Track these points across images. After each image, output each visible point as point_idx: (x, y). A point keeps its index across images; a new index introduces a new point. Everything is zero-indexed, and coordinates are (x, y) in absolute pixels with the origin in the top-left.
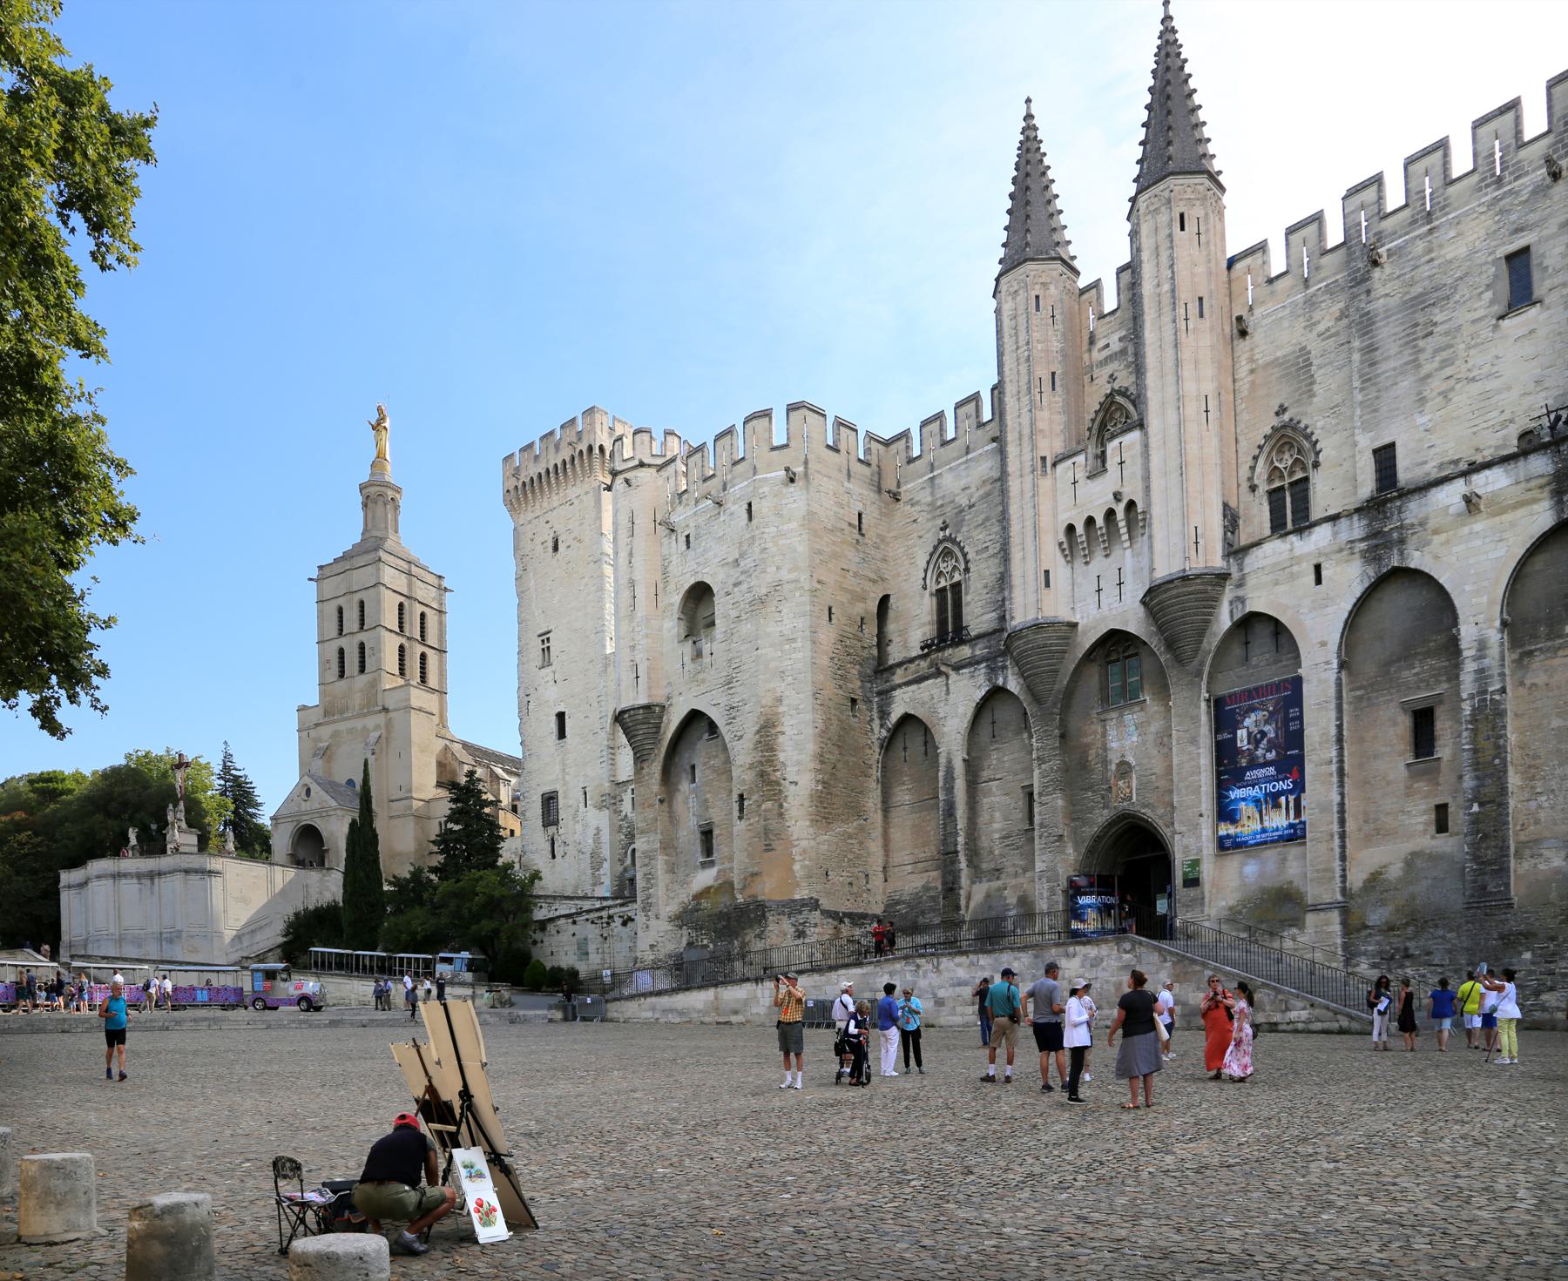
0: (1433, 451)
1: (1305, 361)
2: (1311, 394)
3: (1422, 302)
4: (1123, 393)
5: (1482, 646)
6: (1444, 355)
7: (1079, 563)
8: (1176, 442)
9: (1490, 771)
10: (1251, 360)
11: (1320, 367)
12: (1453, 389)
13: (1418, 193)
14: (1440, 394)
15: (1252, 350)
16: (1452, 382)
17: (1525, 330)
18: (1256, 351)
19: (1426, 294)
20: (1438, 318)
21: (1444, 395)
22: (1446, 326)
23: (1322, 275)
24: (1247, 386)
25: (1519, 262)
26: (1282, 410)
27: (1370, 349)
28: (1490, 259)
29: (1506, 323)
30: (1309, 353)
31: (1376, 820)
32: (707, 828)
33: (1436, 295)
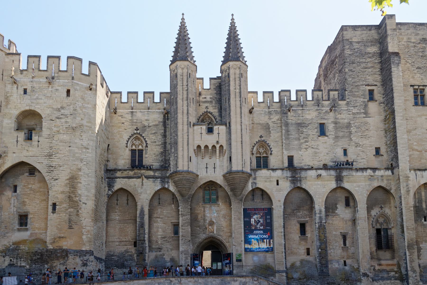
1: (268, 127)
3: (301, 125)
5: (320, 211)
6: (306, 139)
7: (200, 158)
8: (240, 134)
9: (323, 242)
10: (252, 120)
11: (272, 130)
12: (308, 148)
14: (305, 148)
15: (253, 118)
17: (324, 141)
18: (254, 119)
20: (305, 130)
21: (306, 149)
22: (306, 133)
23: (273, 107)
26: (261, 137)
27: (287, 131)
28: (317, 122)
29: (320, 138)
31: (291, 250)
32: (26, 214)
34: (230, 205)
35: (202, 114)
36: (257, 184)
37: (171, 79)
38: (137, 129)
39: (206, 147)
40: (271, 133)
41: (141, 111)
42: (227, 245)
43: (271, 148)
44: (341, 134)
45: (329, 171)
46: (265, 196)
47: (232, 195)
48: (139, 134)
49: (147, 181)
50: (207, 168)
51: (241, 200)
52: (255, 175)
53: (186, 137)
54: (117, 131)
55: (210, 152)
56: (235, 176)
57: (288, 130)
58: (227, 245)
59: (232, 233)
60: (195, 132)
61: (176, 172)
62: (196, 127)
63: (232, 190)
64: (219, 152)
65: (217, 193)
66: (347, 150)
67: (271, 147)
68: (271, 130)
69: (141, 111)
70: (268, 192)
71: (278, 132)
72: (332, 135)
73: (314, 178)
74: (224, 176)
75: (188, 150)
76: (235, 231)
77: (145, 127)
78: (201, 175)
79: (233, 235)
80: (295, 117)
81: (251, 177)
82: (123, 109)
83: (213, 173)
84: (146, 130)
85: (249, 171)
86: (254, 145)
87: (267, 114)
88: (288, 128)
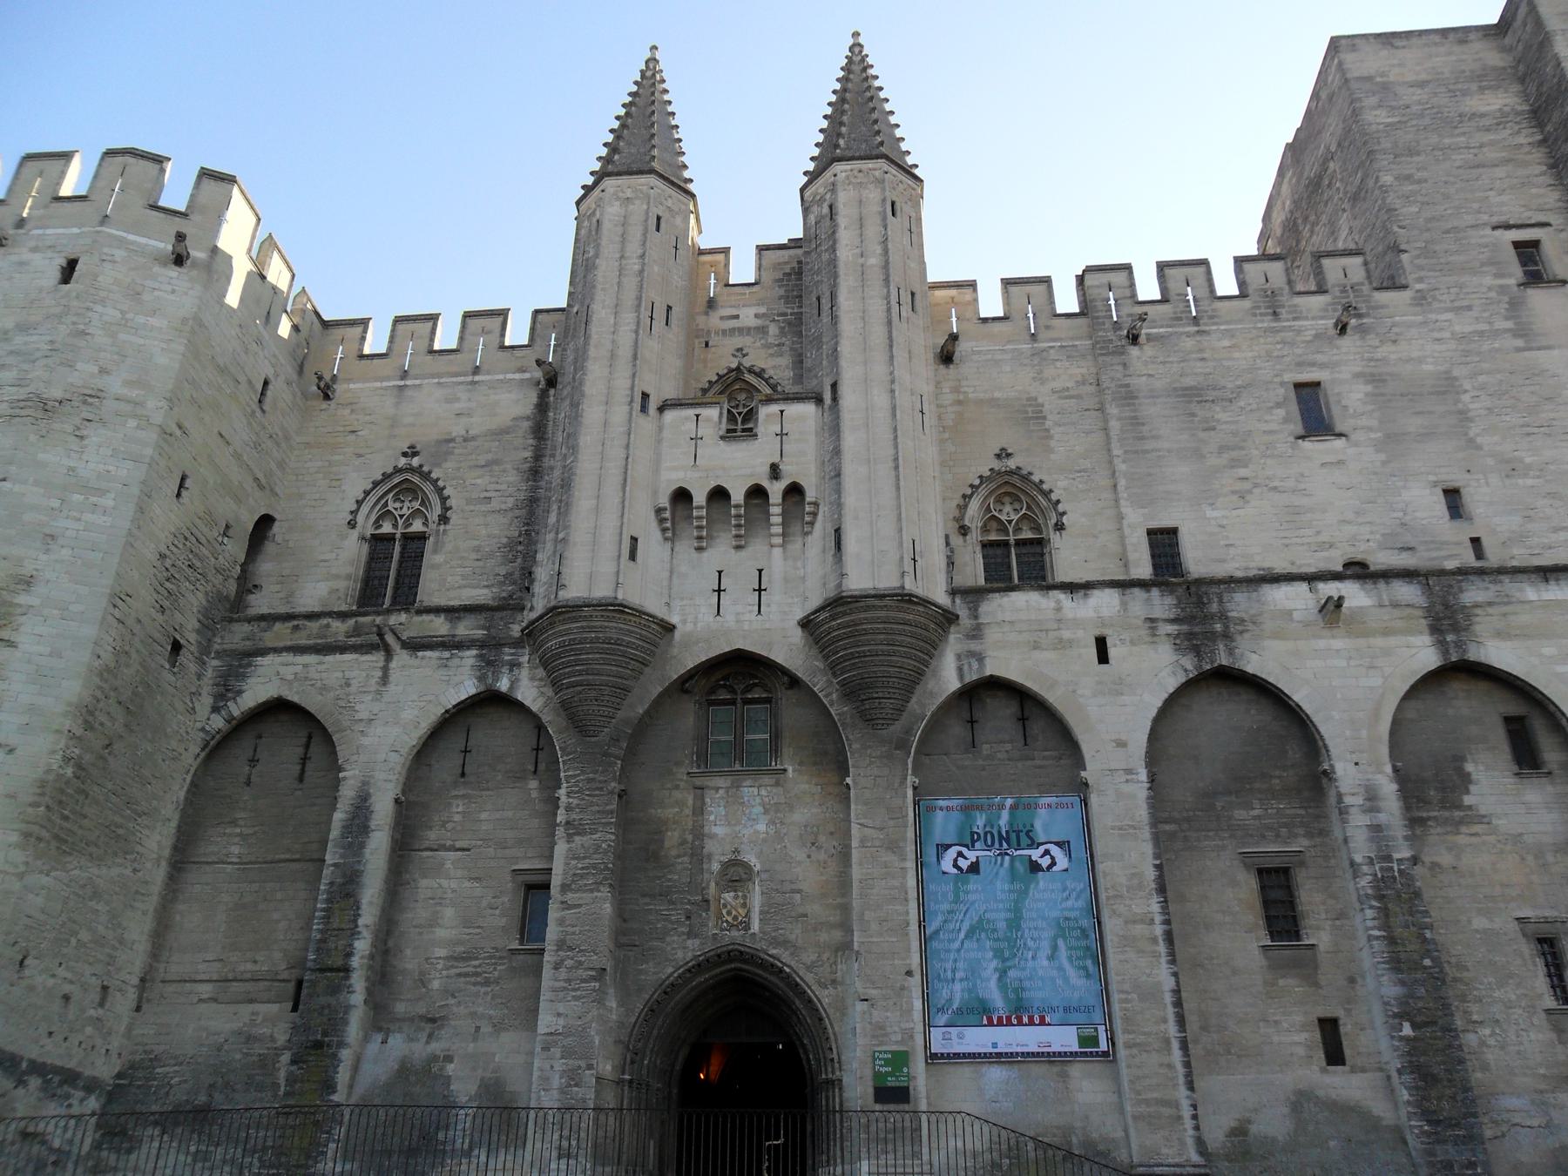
0: (1232, 551)
1: (1033, 412)
2: (1051, 451)
4: (759, 374)
6: (1234, 454)
7: (685, 548)
10: (956, 390)
13: (1179, 295)
14: (1233, 492)
16: (1247, 486)
19: (1202, 389)
24: (953, 416)
25: (1308, 392)
26: (1003, 454)
27: (1136, 422)
28: (1277, 380)
29: (1306, 445)
30: (1043, 406)
33: (1214, 393)
34: (843, 770)
35: (715, 378)
36: (988, 661)
37: (575, 248)
38: (412, 452)
39: (719, 495)
40: (1050, 437)
41: (439, 383)
42: (826, 1001)
43: (1058, 502)
44: (1413, 424)
45: (1382, 585)
46: (1037, 726)
47: (848, 720)
48: (418, 470)
49: (416, 662)
50: (719, 591)
51: (903, 745)
52: (976, 617)
53: (616, 452)
54: (320, 464)
55: (738, 516)
56: (862, 615)
57: (1135, 418)
58: (824, 997)
59: (849, 931)
60: (666, 434)
61: (560, 612)
62: (670, 415)
63: (851, 692)
64: (784, 514)
65: (775, 715)
66: (1464, 492)
67: (1054, 497)
68: (1048, 424)
69: (442, 380)
70: (1052, 697)
71: (1087, 433)
72: (1370, 429)
73: (1307, 624)
74: (805, 624)
75: (623, 507)
76: (868, 915)
77: (452, 440)
78: (689, 627)
79: (857, 938)
80: (1163, 363)
81: (953, 629)
82: (365, 380)
83: (753, 616)
84: (452, 453)
85: (941, 597)
86: (969, 491)
87: (1026, 361)
88: (1135, 411)
